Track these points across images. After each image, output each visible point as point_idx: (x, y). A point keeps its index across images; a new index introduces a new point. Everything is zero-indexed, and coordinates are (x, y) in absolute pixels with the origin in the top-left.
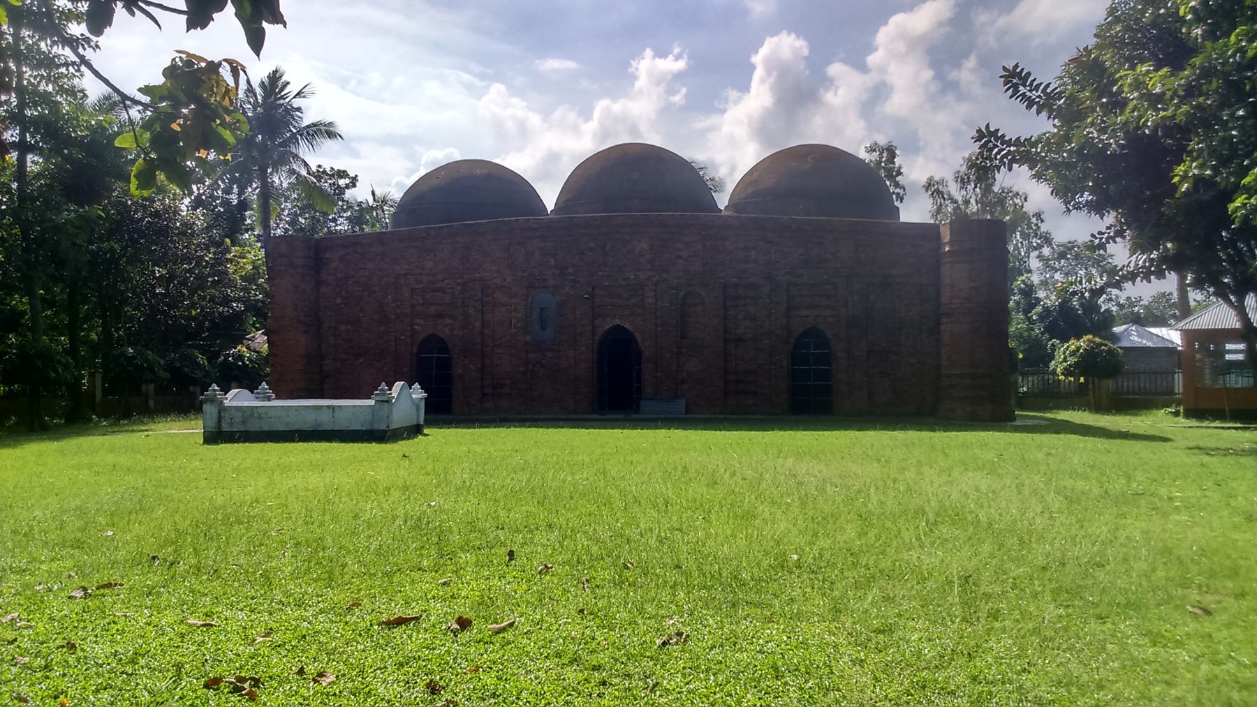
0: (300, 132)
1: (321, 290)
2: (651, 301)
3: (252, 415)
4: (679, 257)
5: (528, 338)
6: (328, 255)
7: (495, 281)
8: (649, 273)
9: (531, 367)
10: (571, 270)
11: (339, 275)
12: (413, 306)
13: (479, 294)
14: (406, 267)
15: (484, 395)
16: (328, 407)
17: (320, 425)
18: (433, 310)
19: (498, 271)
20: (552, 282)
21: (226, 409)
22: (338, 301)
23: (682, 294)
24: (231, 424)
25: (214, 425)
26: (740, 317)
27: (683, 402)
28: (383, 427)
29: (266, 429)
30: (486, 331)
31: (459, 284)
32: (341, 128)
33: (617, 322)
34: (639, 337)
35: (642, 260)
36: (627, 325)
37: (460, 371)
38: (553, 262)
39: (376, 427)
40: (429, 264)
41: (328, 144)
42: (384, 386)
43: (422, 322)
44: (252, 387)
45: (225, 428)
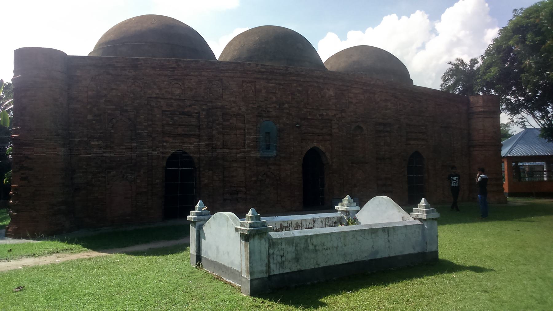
3: (306, 248)
4: (351, 103)
5: (258, 155)
7: (234, 109)
10: (286, 106)
11: (90, 93)
12: (163, 126)
14: (157, 91)
15: (225, 200)
17: (377, 252)
18: (180, 130)
19: (234, 102)
20: (274, 114)
21: (272, 243)
22: (90, 117)
25: (264, 268)
29: (323, 264)
30: (225, 149)
31: (203, 110)
33: (315, 144)
34: (328, 155)
36: (321, 147)
37: (206, 181)
38: (274, 99)
40: (178, 92)
43: (171, 140)
45: (276, 270)
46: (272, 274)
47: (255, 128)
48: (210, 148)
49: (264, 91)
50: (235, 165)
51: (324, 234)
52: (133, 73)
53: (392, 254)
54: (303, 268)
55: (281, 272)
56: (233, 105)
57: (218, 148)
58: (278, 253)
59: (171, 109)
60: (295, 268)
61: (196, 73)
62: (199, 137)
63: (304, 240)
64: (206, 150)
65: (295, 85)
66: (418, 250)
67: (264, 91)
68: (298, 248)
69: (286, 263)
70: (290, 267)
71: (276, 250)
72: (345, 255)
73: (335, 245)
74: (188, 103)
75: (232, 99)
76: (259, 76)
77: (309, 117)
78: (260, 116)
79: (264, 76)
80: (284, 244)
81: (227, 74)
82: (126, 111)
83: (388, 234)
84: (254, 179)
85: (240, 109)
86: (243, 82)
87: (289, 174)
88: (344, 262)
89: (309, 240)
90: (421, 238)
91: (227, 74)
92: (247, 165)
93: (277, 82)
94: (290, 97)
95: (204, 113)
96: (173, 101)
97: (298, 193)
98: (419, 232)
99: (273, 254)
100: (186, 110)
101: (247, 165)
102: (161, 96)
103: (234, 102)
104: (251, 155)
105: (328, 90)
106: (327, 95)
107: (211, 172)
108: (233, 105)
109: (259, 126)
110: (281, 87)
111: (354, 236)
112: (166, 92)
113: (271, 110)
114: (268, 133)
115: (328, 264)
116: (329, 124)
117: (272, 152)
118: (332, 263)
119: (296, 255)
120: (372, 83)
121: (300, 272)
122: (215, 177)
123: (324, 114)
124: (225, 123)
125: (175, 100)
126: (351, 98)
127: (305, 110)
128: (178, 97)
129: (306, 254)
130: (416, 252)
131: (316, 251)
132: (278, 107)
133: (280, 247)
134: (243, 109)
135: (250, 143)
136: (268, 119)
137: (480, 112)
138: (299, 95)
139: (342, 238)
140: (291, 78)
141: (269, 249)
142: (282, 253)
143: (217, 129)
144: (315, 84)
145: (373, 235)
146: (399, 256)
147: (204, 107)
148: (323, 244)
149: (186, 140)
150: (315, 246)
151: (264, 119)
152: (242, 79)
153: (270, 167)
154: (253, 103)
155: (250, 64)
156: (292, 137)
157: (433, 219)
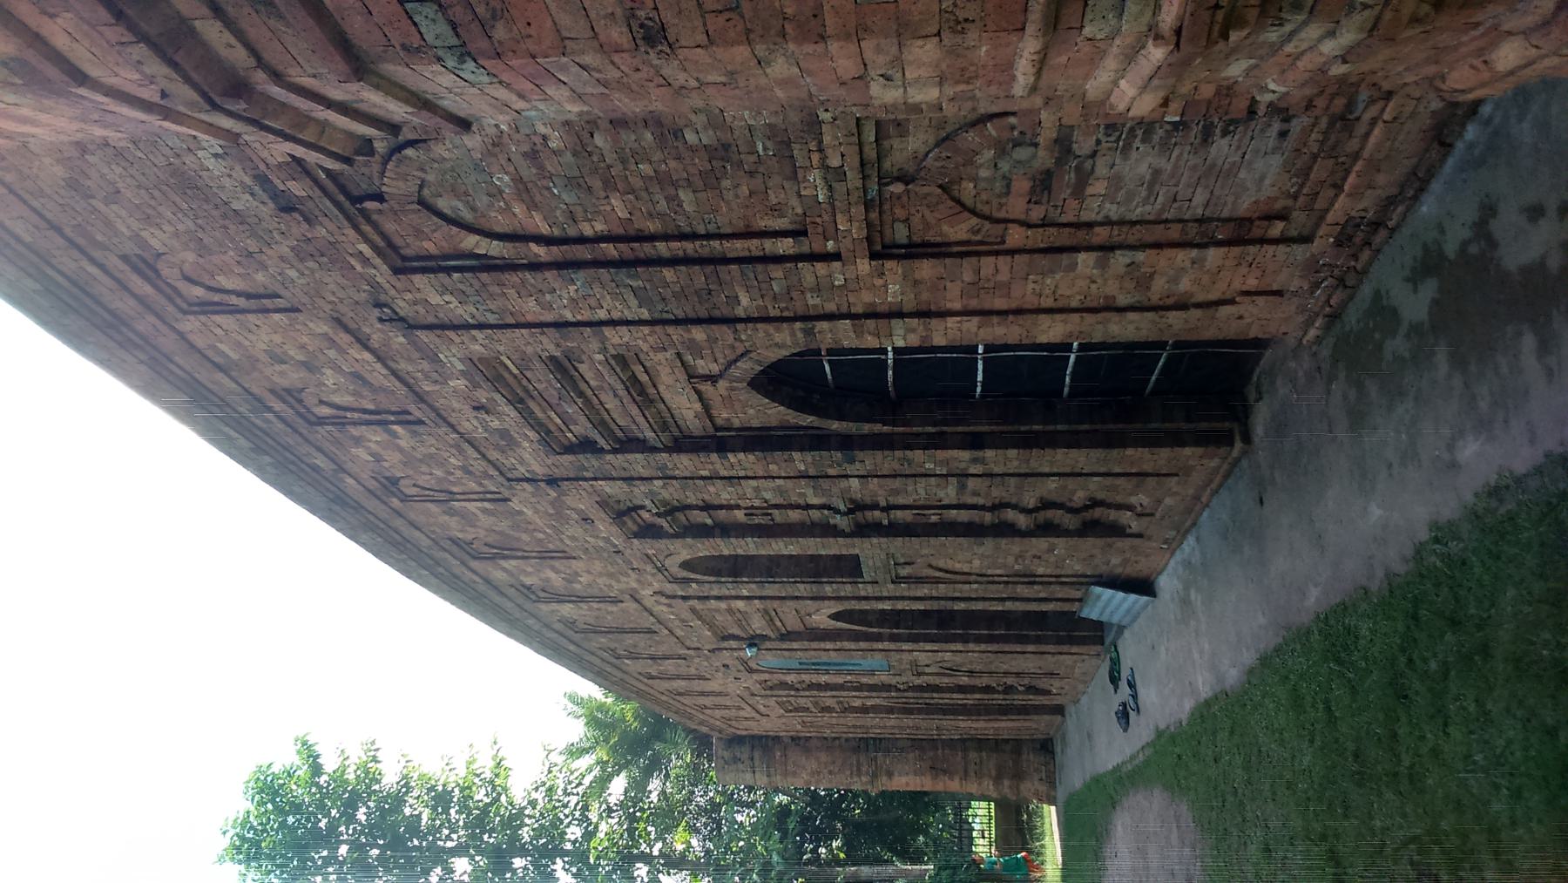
26: (757, 503)
86: (652, 678)
144: (558, 626)
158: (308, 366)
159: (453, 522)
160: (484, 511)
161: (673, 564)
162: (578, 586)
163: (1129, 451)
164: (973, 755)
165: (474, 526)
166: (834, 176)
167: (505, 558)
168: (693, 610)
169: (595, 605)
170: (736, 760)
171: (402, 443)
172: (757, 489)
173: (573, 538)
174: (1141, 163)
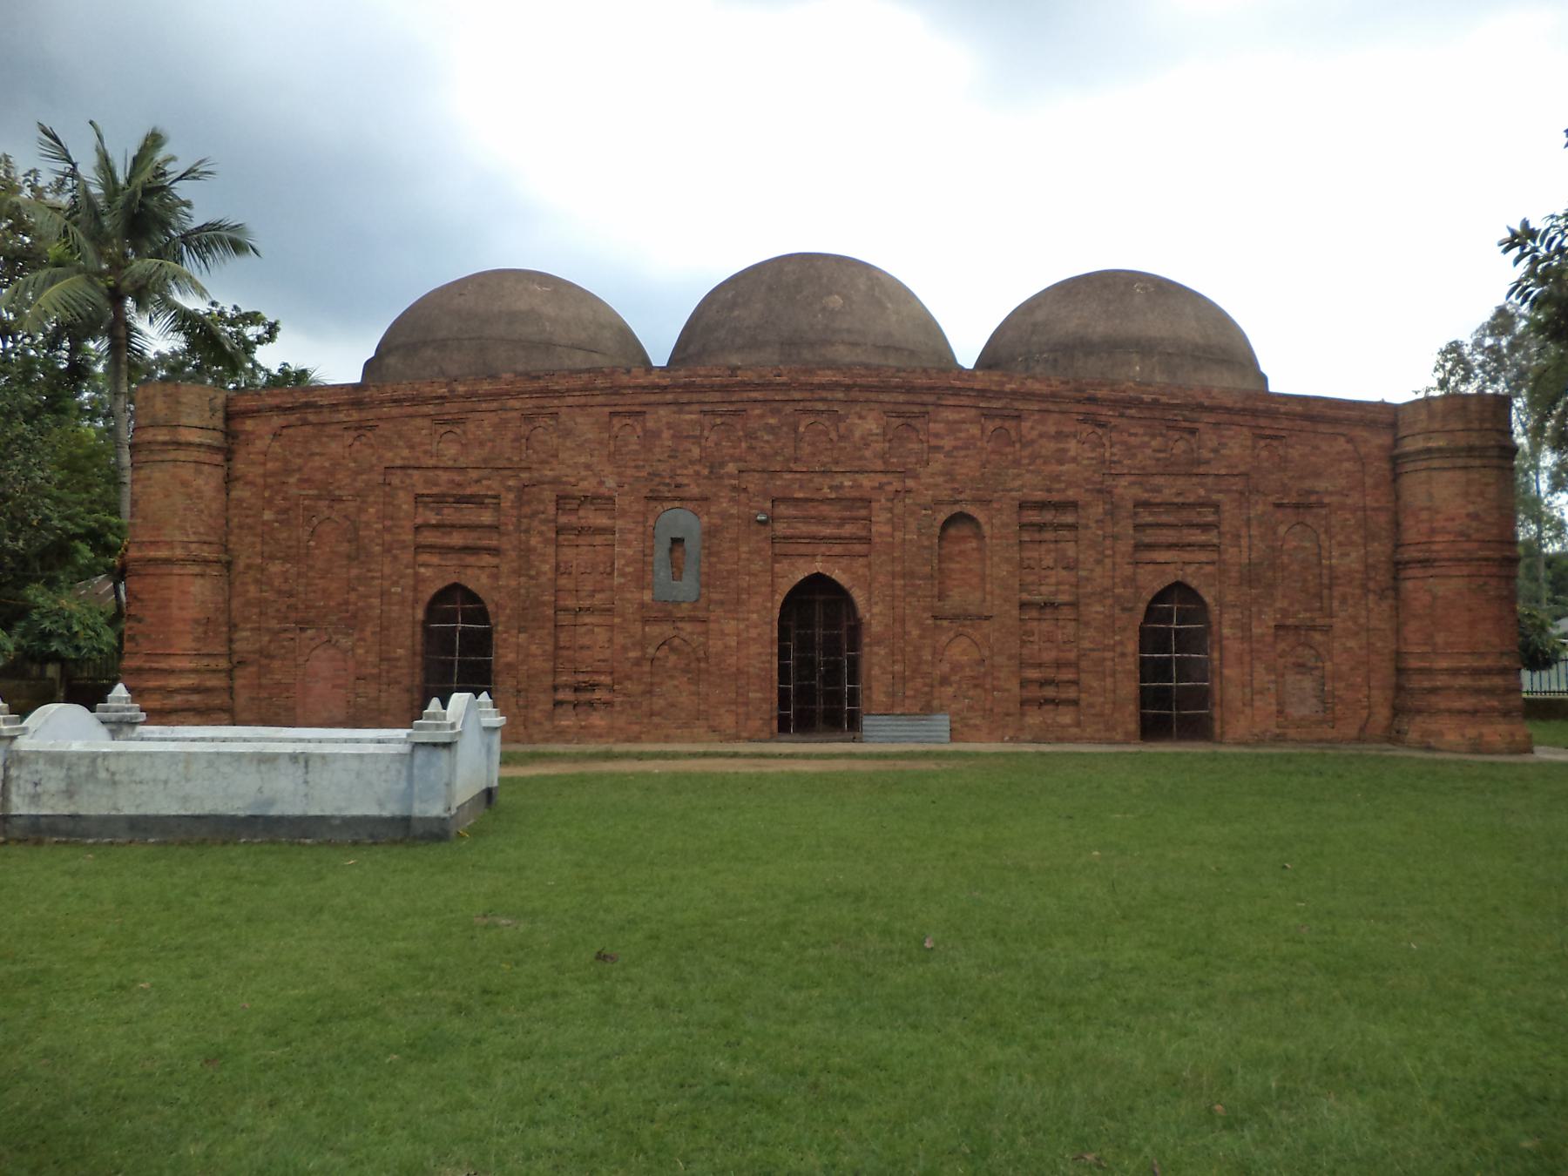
0: (185, 238)
1: (234, 494)
2: (887, 529)
3: (92, 776)
4: (938, 448)
5: (647, 596)
6: (249, 425)
8: (884, 479)
9: (651, 651)
10: (731, 468)
11: (270, 465)
12: (418, 529)
13: (551, 509)
15: (558, 704)
16: (294, 757)
17: (271, 802)
18: (457, 539)
19: (588, 467)
20: (694, 490)
23: (942, 517)
24: (35, 798)
27: (942, 723)
28: (436, 810)
30: (563, 581)
31: (509, 489)
32: (257, 236)
33: (818, 567)
34: (859, 596)
35: (868, 453)
36: (838, 575)
37: (511, 657)
38: (696, 452)
39: (419, 810)
40: (452, 450)
41: (236, 263)
42: (435, 702)
43: (435, 560)
44: (90, 695)
46: (14, 812)
47: (640, 529)
48: (523, 579)
49: (666, 434)
50: (588, 620)
51: (136, 753)
52: (355, 416)
53: (314, 811)
54: (82, 812)
55: (33, 812)
56: (583, 473)
57: (543, 579)
58: (28, 777)
59: (435, 490)
60: (63, 808)
61: (495, 405)
62: (495, 551)
63: (87, 761)
64: (513, 583)
65: (757, 412)
66: (391, 810)
67: (666, 434)
68: (74, 774)
69: (45, 798)
70: (53, 806)
71: (25, 774)
72: (185, 799)
73: (163, 777)
74: (474, 474)
75: (582, 460)
76: (653, 398)
77: (801, 495)
78: (655, 499)
79: (669, 397)
80: (41, 762)
81: (570, 401)
82: (340, 500)
83: (306, 766)
84: (632, 654)
85: (601, 483)
87: (734, 644)
88: (183, 812)
89: (100, 760)
90: (403, 785)
91: (570, 401)
92: (617, 620)
93: (706, 408)
94: (744, 445)
95: (511, 496)
96: (440, 472)
97: (759, 695)
98: (399, 772)
99: (18, 777)
100: (468, 491)
101: (617, 620)
102: (412, 463)
103: (588, 467)
104: (629, 596)
105: (860, 417)
106: (857, 434)
107: (522, 636)
108: (583, 473)
109: (651, 522)
110: (718, 421)
111: (210, 764)
112: (426, 452)
113: (686, 481)
114: (677, 542)
115: (142, 811)
116: (863, 513)
117: (687, 588)
118: (150, 810)
119: (68, 785)
120: (1008, 387)
121: (73, 817)
122: (533, 647)
123: (847, 483)
124: (563, 520)
125: (446, 469)
126: (937, 436)
127: (788, 476)
128: (450, 463)
129: (90, 787)
130: (386, 813)
131: (114, 783)
132: (706, 472)
133: (33, 767)
134: (611, 483)
135: (627, 565)
136: (677, 504)
137: (1419, 452)
138: (770, 438)
139: (181, 767)
140: (745, 396)
141: (6, 769)
142: (36, 778)
143: (541, 533)
144: (820, 406)
145: (263, 768)
146: (332, 817)
147: (510, 483)
148: (131, 772)
149: (471, 560)
150: (113, 774)
151: (668, 505)
152: (607, 410)
153: (679, 625)
154: (636, 467)
155: (628, 371)
156: (744, 548)
157: (435, 745)
158: (1215, 451)
159: (1052, 430)
160: (1065, 451)
161: (970, 509)
162: (911, 446)
163: (1132, 708)
164: (223, 664)
165: (1041, 436)
166: (1313, 619)
167: (983, 431)
168: (867, 502)
169: (879, 447)
170: (213, 410)
171: (1149, 452)
172: (1092, 571)
173: (1019, 475)
174: (1308, 683)
